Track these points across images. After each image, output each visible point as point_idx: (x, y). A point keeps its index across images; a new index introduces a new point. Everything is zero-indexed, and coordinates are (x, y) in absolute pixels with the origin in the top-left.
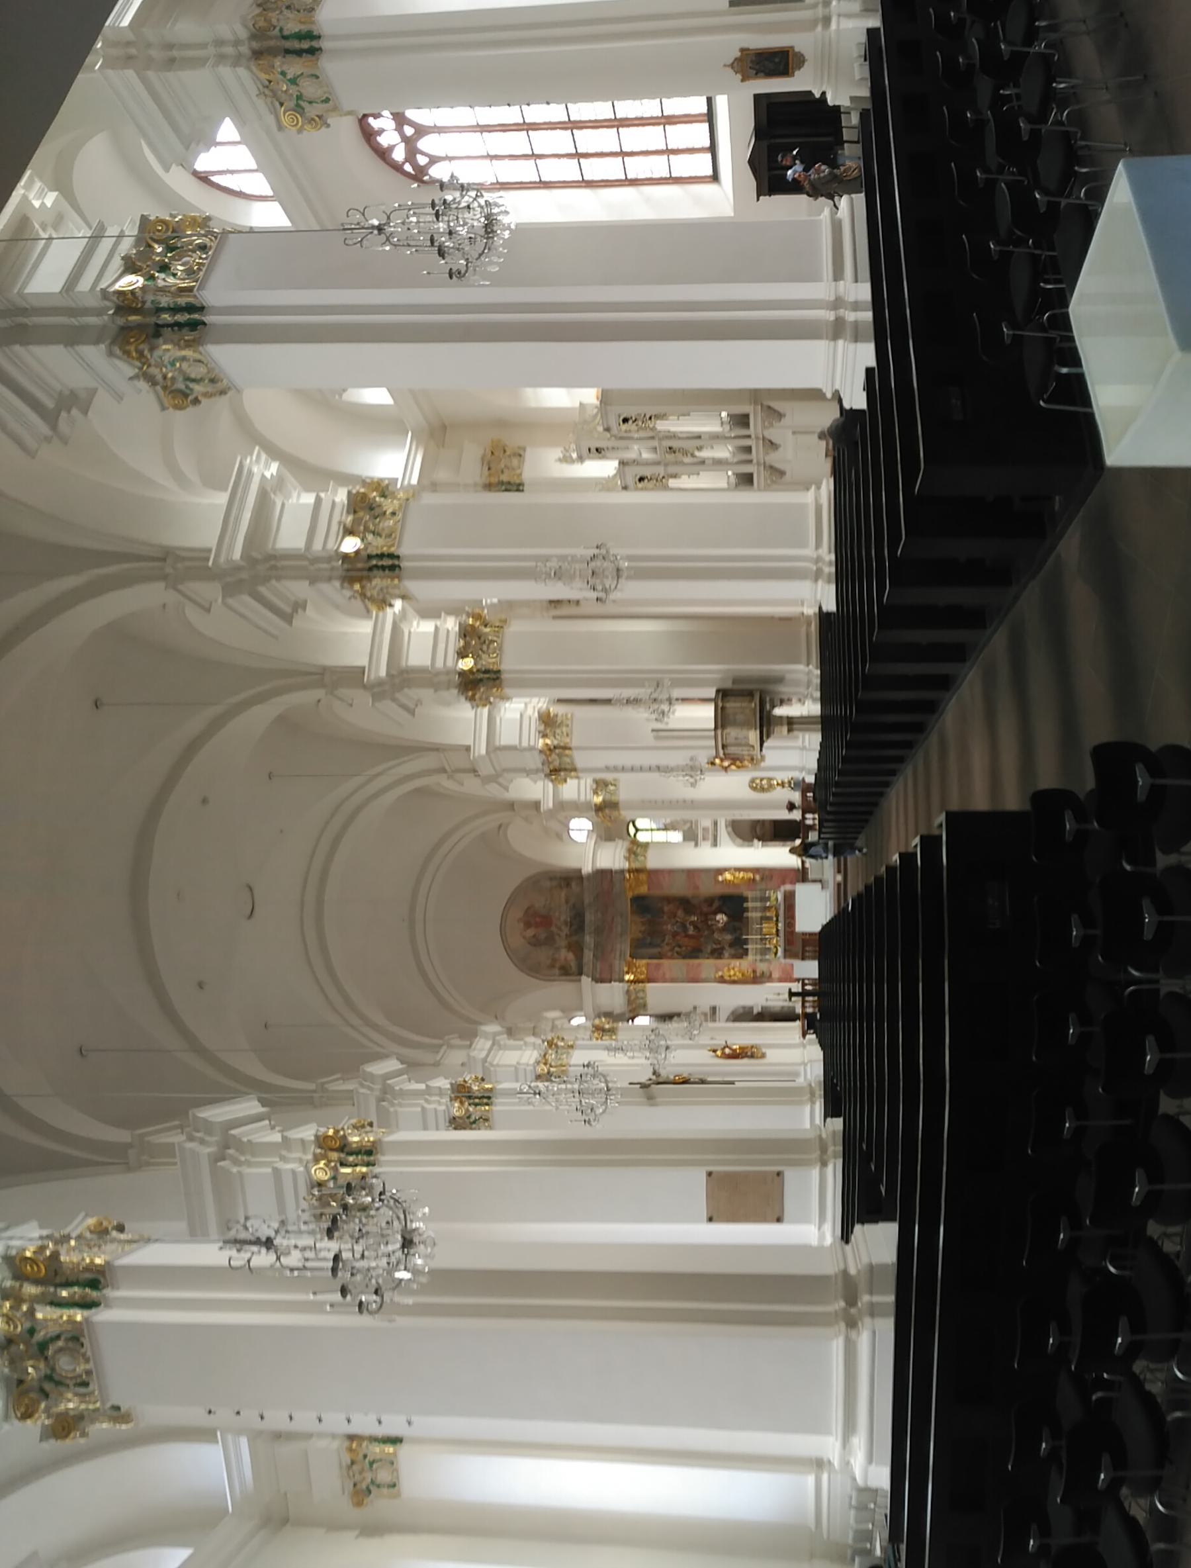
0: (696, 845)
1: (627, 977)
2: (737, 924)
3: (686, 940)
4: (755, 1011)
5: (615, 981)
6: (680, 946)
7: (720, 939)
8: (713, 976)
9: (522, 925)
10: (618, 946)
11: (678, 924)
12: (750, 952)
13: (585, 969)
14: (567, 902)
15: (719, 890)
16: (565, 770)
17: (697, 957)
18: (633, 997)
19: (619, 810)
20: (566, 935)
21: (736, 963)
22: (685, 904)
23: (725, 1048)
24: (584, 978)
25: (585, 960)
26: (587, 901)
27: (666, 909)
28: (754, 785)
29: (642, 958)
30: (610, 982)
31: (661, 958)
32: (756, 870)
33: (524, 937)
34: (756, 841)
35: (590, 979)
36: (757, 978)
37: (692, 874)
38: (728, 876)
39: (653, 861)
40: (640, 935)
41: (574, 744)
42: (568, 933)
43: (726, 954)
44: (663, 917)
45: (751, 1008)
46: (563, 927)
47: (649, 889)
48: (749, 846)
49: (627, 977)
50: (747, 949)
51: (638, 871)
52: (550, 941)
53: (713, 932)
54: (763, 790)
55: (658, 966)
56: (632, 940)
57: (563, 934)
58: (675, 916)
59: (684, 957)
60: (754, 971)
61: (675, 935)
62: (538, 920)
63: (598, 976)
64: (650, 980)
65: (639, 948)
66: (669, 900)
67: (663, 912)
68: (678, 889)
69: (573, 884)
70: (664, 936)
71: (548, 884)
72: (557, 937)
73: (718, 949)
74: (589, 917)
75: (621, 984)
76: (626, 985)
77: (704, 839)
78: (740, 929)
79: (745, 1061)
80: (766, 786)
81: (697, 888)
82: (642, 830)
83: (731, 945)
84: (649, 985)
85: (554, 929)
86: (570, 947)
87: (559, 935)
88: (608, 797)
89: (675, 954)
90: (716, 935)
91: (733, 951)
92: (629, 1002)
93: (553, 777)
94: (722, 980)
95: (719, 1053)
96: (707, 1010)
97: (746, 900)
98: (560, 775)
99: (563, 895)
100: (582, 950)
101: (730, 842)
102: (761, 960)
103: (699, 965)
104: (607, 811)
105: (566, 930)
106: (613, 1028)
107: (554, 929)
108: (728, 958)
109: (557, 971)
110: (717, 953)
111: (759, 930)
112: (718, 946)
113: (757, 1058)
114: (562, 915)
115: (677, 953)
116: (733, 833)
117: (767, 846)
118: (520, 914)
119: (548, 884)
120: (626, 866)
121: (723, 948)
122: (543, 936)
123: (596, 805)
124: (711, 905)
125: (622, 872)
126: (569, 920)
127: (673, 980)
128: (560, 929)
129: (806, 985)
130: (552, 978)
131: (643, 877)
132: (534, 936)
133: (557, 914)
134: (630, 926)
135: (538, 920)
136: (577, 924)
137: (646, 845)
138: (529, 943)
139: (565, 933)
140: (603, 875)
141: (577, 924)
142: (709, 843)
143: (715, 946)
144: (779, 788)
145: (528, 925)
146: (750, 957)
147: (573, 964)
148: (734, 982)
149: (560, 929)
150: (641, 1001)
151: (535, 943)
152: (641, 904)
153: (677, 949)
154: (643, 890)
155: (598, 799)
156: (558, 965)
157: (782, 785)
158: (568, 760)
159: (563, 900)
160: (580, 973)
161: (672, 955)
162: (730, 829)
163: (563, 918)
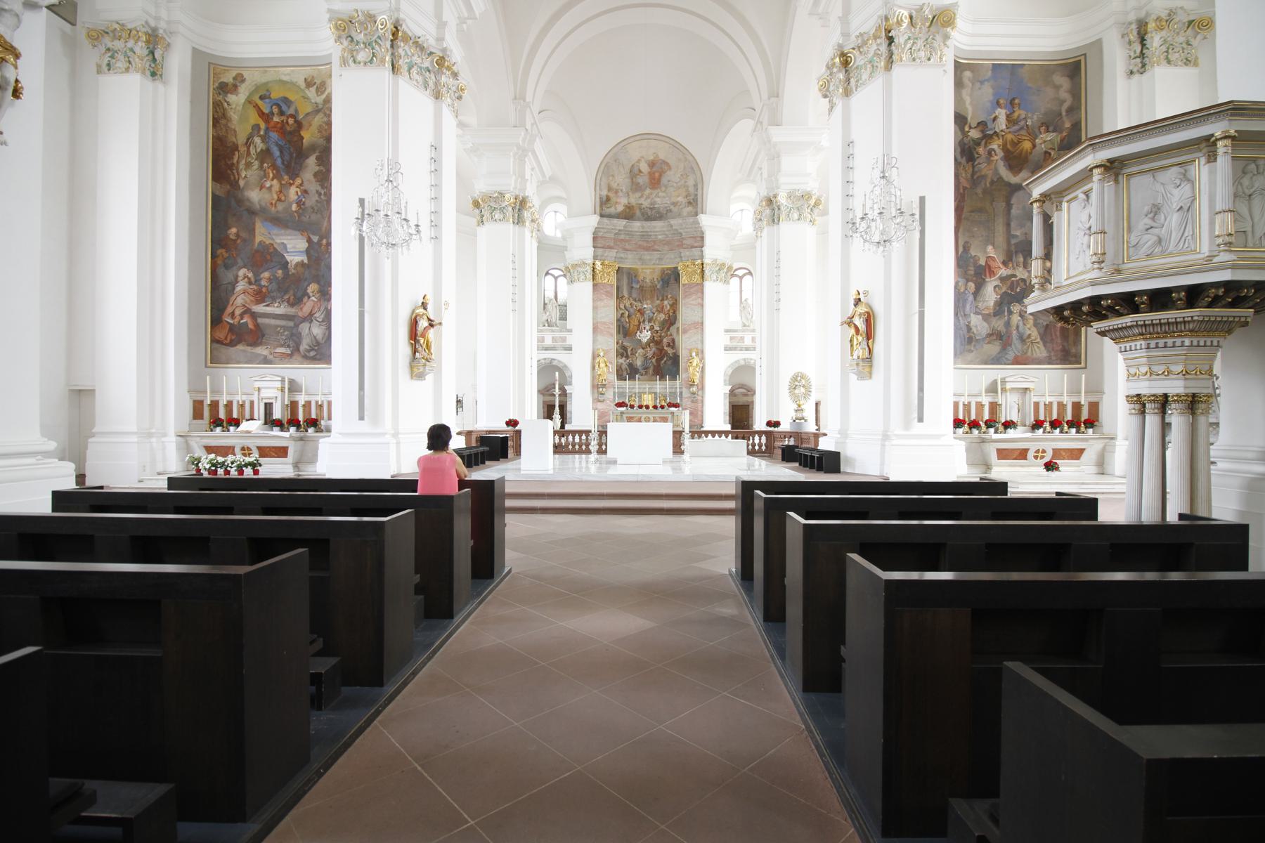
0: (727, 331)
1: (598, 263)
2: (651, 371)
3: (636, 323)
4: (566, 387)
5: (594, 251)
6: (629, 316)
7: (637, 355)
8: (599, 347)
9: (652, 158)
10: (630, 256)
11: (651, 315)
12: (622, 382)
13: (606, 220)
14: (674, 204)
15: (683, 354)
16: (848, 80)
17: (618, 332)
18: (580, 270)
19: (768, 224)
20: (642, 204)
21: (613, 369)
22: (671, 321)
23: (429, 319)
24: (596, 218)
25: (615, 221)
26: (672, 222)
27: (666, 302)
28: (799, 379)
29: (618, 280)
30: (594, 247)
31: (617, 297)
32: (702, 387)
33: (639, 161)
34: (730, 387)
35: (596, 226)
36: (598, 387)
37: (700, 325)
38: (696, 361)
39: (712, 288)
40: (641, 278)
41: (896, 69)
42: (643, 206)
43: (622, 361)
44: (658, 299)
45: (570, 384)
46: (649, 201)
47: (684, 285)
48: (725, 381)
49: (598, 263)
50: (626, 380)
51: (703, 271)
52: (636, 187)
53: (643, 348)
54: (793, 388)
55: (609, 294)
56: (637, 269)
57: (642, 201)
58: (659, 312)
59: (618, 320)
60: (604, 386)
61: (641, 312)
62: (657, 175)
63: (600, 234)
64: (595, 286)
65: (627, 277)
66: (675, 306)
67: (662, 300)
68: (686, 314)
69: (690, 208)
70: (639, 300)
71: (691, 182)
72: (638, 195)
73: (626, 351)
74: (658, 225)
75: (592, 258)
76: (591, 262)
77: (731, 338)
78: (646, 374)
79: (405, 348)
80: (797, 391)
81: (685, 332)
82: (741, 282)
83: (630, 365)
84: (590, 284)
85: (648, 191)
86: (629, 207)
87: (641, 197)
88: (784, 211)
89: (621, 312)
90: (640, 351)
91: (625, 366)
92: (574, 266)
93: (837, 60)
94: (595, 356)
95: (421, 311)
96: (568, 343)
97: (674, 378)
98: (840, 71)
99: (680, 199)
100: (625, 218)
101: (729, 364)
102: (614, 393)
103: (612, 335)
104: (768, 211)
105: (646, 203)
106: (524, 222)
107: (648, 191)
108: (617, 362)
109: (605, 193)
110: (622, 352)
111: (644, 391)
112: (629, 354)
113: (411, 367)
114: (661, 199)
115: (623, 314)
116: (737, 366)
117: (725, 398)
118: (662, 156)
119: (691, 182)
120: (706, 261)
121: (627, 357)
122: (642, 180)
123: (775, 196)
124: (669, 345)
125: (702, 257)
126: (656, 206)
127: (595, 308)
128: (648, 197)
129: (580, 437)
130: (598, 188)
131: (697, 278)
132: (640, 171)
133: (660, 194)
134: (649, 270)
135: (657, 175)
136: (653, 215)
137: (726, 282)
138: (633, 166)
139: (643, 203)
140: (700, 240)
141: (653, 215)
142: (728, 342)
143: (629, 350)
144: (795, 407)
145: (652, 164)
146: (617, 383)
147: (612, 210)
148: (593, 368)
149: (648, 197)
150: (576, 277)
151: (634, 173)
152: (670, 278)
153: (627, 313)
154: (684, 280)
155: (782, 199)
156: (611, 194)
157: (799, 409)
158: (865, 76)
159: (674, 200)
160: (602, 216)
161: (621, 309)
162: (742, 363)
163: (658, 200)
